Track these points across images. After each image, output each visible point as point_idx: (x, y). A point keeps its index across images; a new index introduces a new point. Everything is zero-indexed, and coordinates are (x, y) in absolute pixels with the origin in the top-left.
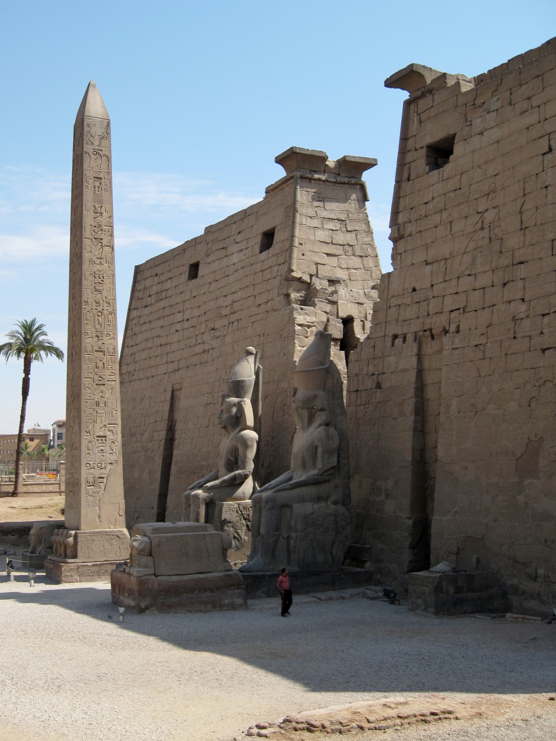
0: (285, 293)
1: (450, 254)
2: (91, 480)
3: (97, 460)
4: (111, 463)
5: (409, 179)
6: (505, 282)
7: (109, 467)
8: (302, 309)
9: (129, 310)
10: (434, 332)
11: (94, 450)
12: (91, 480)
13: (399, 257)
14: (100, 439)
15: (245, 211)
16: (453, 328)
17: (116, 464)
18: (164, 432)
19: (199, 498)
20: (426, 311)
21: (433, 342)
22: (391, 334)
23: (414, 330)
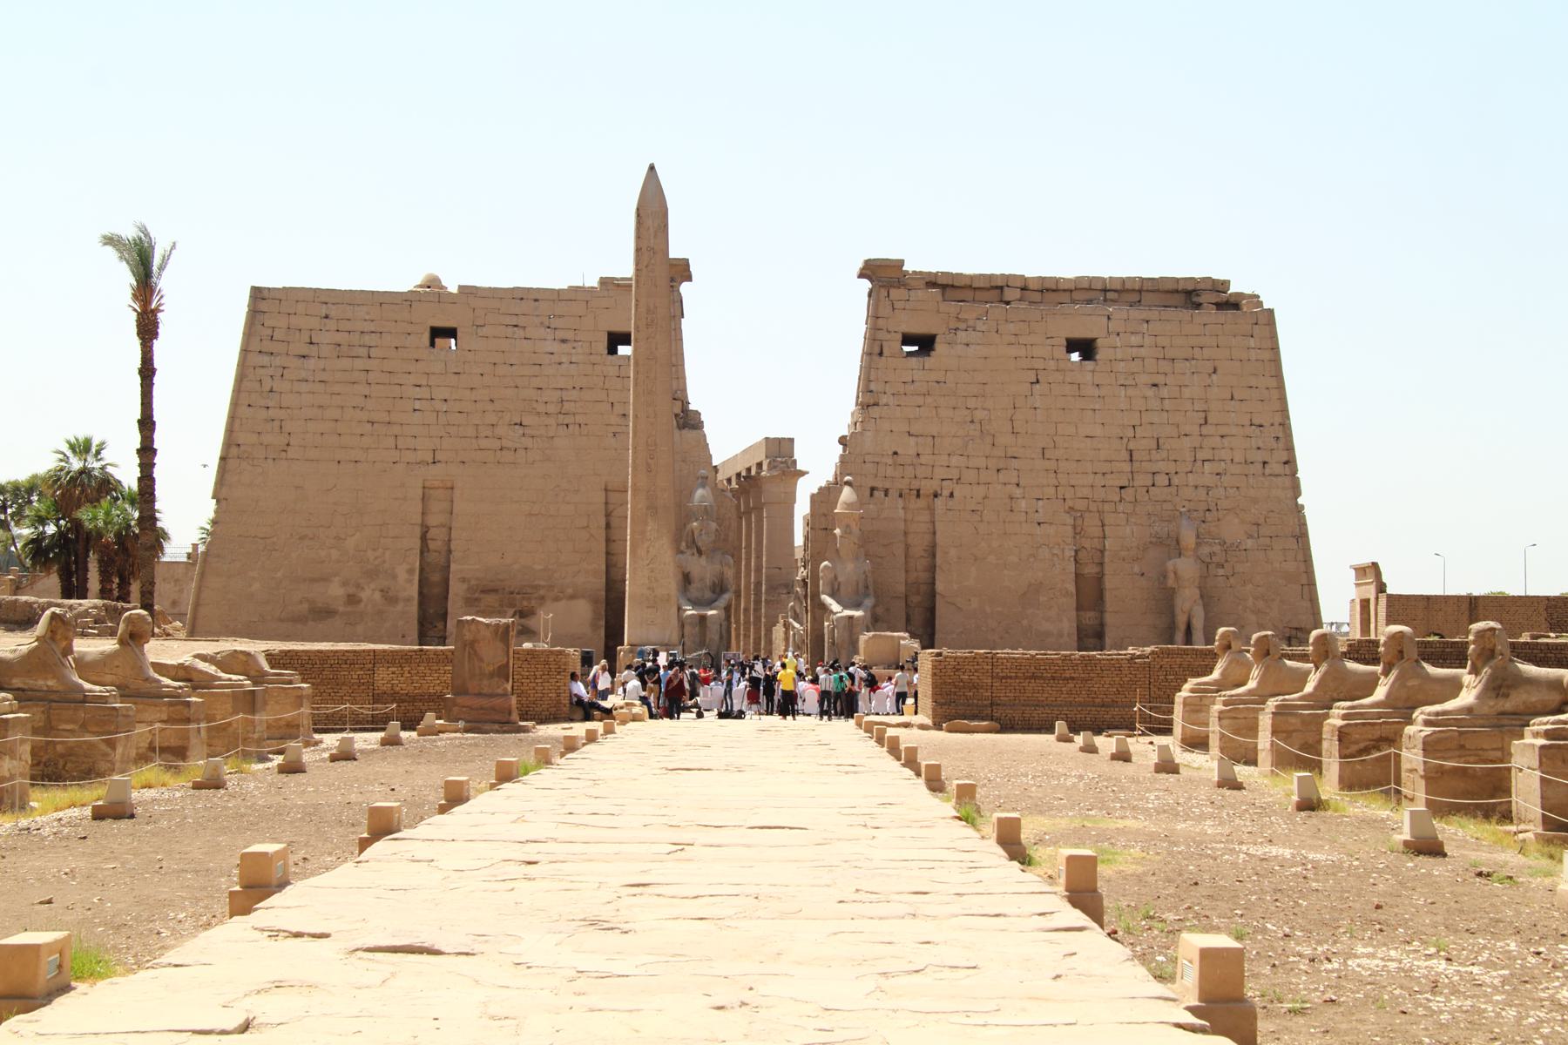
5: (881, 354)
16: (946, 493)
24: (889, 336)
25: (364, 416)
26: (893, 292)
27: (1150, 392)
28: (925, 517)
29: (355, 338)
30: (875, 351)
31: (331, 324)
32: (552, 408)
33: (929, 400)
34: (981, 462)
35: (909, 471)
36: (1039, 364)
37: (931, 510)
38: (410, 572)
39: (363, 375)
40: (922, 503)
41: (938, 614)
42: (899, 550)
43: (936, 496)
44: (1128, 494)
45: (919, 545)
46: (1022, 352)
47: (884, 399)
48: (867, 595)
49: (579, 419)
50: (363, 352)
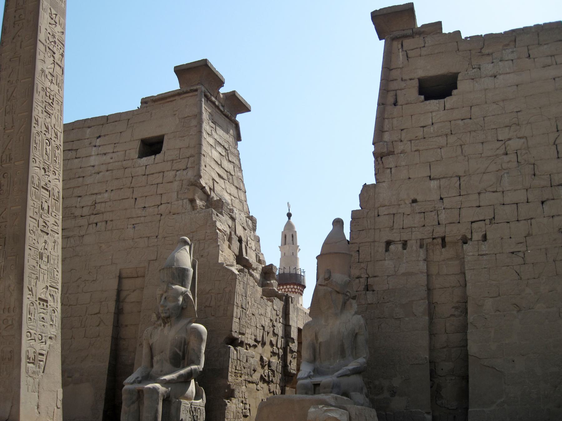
0: (191, 197)
1: (465, 172)
3: (38, 330)
4: (50, 338)
6: (544, 200)
7: (49, 342)
8: (217, 215)
10: (446, 239)
11: (36, 315)
13: (389, 170)
14: (42, 303)
16: (477, 236)
17: (55, 340)
19: (158, 393)
20: (437, 220)
21: (443, 250)
22: (385, 239)
23: (420, 237)
32: (86, 211)
40: (448, 252)
41: (470, 380)
42: (420, 307)
43: (465, 241)
49: (107, 217)
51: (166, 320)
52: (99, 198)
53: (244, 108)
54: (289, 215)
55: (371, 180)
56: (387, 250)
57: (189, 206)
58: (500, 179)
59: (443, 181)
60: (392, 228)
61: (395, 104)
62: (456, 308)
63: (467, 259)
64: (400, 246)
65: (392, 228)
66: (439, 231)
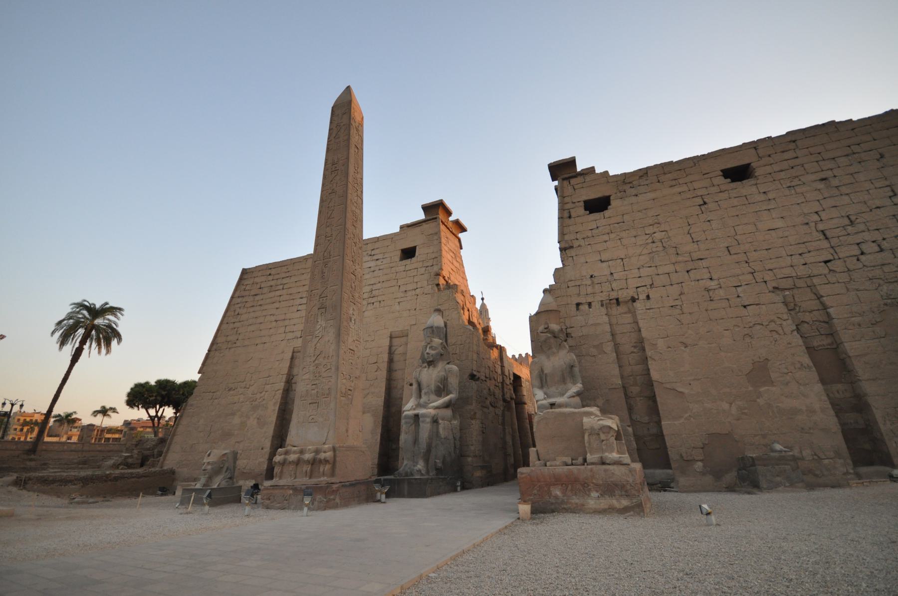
2: (344, 391)
5: (570, 217)
9: (232, 297)
12: (344, 391)
15: (378, 238)
16: (642, 297)
18: (283, 384)
24: (573, 206)
25: (273, 318)
26: (573, 181)
27: (821, 186)
28: (628, 318)
29: (279, 282)
30: (565, 216)
31: (270, 278)
33: (612, 236)
34: (670, 268)
35: (606, 287)
36: (699, 193)
37: (633, 312)
38: (275, 404)
39: (278, 299)
40: (622, 309)
41: (658, 399)
42: (609, 348)
43: (634, 300)
44: (837, 265)
45: (627, 342)
46: (685, 188)
47: (576, 244)
48: (574, 383)
49: (380, 298)
50: (281, 287)
51: (431, 363)
52: (375, 287)
53: (463, 229)
54: (483, 299)
55: (560, 265)
56: (578, 309)
57: (436, 288)
58: (652, 259)
59: (610, 262)
60: (579, 295)
61: (570, 217)
62: (635, 347)
63: (638, 312)
64: (587, 307)
65: (579, 295)
66: (614, 295)
